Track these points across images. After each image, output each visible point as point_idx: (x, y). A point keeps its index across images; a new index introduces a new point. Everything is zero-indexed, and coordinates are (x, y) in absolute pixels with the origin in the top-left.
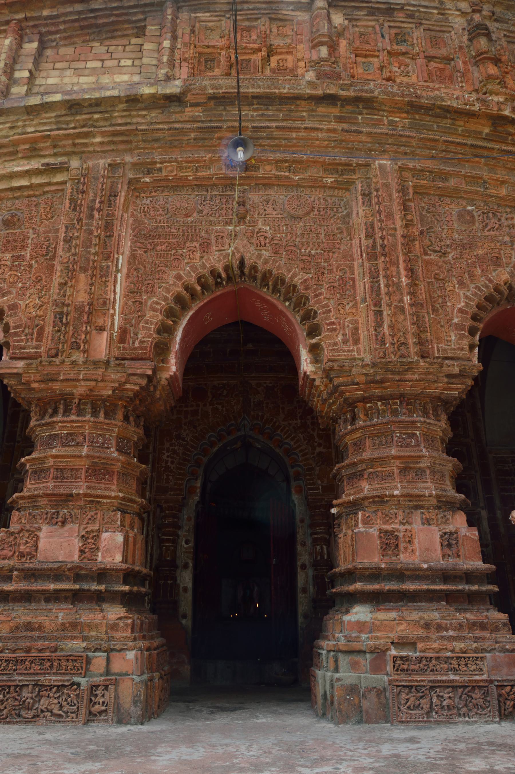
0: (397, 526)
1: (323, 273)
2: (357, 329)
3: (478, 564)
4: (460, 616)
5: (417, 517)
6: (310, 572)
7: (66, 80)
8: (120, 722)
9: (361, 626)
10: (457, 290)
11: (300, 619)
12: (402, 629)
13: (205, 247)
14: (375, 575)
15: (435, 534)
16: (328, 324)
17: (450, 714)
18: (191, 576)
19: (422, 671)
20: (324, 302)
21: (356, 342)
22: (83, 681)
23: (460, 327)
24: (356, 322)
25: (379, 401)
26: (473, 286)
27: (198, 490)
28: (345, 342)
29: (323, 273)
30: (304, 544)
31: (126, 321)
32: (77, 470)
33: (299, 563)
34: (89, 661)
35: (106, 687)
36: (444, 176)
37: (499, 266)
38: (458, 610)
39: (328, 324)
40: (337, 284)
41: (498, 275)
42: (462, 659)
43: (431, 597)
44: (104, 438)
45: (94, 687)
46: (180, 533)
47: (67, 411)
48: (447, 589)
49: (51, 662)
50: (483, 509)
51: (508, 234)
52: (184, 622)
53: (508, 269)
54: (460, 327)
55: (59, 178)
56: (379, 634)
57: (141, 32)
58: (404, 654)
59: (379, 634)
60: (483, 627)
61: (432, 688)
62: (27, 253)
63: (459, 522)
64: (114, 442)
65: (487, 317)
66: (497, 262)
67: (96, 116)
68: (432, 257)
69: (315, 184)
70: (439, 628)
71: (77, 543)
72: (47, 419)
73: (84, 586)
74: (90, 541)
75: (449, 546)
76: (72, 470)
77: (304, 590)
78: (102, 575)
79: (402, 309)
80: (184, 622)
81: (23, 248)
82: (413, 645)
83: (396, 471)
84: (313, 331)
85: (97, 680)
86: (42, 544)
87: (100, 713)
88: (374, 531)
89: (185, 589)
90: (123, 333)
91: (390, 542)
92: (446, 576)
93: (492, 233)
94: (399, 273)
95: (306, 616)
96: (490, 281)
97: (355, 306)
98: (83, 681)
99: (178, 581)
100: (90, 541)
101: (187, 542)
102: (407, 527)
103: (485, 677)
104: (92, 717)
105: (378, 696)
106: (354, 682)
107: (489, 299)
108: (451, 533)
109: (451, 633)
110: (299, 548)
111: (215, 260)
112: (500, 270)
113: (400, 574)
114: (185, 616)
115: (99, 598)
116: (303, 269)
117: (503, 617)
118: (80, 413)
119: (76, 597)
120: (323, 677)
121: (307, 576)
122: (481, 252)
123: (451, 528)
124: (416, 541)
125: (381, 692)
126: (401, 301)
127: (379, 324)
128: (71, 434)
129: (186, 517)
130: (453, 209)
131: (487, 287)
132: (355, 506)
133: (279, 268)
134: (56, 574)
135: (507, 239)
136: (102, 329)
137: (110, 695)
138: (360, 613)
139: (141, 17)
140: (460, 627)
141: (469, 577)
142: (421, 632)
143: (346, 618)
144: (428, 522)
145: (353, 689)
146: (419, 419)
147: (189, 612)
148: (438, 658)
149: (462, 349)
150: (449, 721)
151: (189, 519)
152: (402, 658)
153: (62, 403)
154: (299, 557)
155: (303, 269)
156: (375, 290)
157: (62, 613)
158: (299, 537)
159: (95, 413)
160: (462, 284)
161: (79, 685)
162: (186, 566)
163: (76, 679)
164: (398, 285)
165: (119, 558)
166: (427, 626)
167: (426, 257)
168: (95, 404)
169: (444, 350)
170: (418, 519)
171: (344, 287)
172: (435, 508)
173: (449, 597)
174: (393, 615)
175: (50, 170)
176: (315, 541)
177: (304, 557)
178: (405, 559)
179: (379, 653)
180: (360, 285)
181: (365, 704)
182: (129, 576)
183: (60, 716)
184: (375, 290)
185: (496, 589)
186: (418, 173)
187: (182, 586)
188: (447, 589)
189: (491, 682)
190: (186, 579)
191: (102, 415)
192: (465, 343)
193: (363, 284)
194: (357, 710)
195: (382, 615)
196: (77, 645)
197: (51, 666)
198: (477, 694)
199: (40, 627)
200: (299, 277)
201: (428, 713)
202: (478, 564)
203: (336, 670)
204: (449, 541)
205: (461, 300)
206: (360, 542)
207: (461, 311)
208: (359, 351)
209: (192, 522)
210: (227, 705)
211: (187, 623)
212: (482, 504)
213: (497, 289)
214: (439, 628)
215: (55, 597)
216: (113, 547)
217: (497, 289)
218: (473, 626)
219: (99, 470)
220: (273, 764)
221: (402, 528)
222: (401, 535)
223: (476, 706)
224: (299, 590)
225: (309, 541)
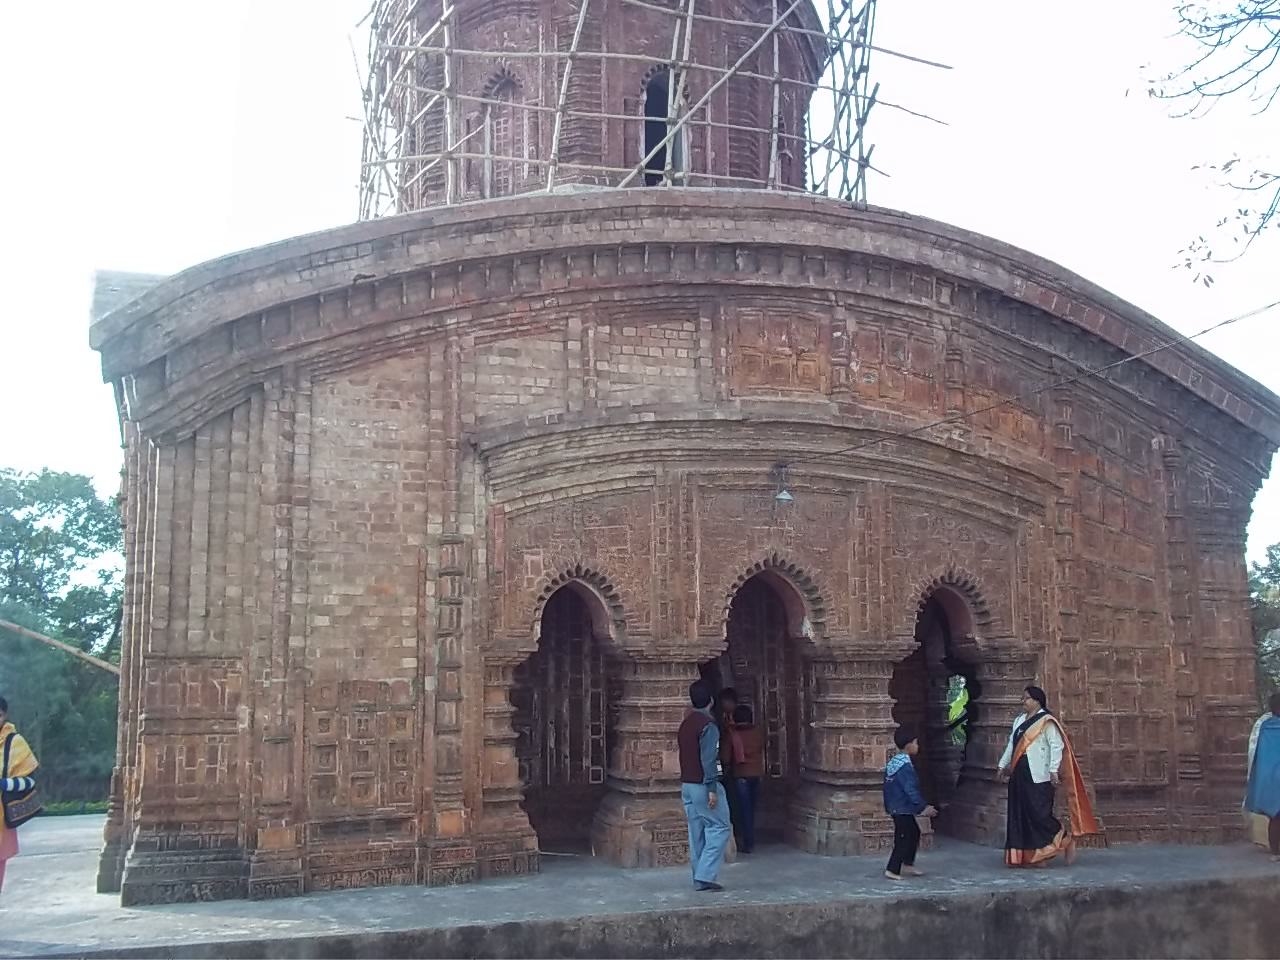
7: (635, 369)
12: (867, 807)
13: (751, 546)
14: (850, 775)
19: (875, 829)
21: (847, 623)
36: (912, 490)
53: (943, 566)
55: (648, 482)
57: (694, 317)
62: (628, 547)
67: (677, 431)
69: (827, 492)
81: (625, 542)
82: (871, 815)
84: (819, 612)
90: (702, 615)
91: (859, 755)
111: (758, 557)
113: (864, 775)
120: (817, 831)
125: (855, 840)
130: (916, 514)
138: (841, 798)
139: (694, 305)
145: (841, 839)
171: (842, 581)
174: (859, 798)
175: (642, 476)
178: (867, 766)
186: (896, 487)
193: (854, 580)
195: (854, 799)
205: (915, 590)
207: (912, 600)
217: (935, 582)
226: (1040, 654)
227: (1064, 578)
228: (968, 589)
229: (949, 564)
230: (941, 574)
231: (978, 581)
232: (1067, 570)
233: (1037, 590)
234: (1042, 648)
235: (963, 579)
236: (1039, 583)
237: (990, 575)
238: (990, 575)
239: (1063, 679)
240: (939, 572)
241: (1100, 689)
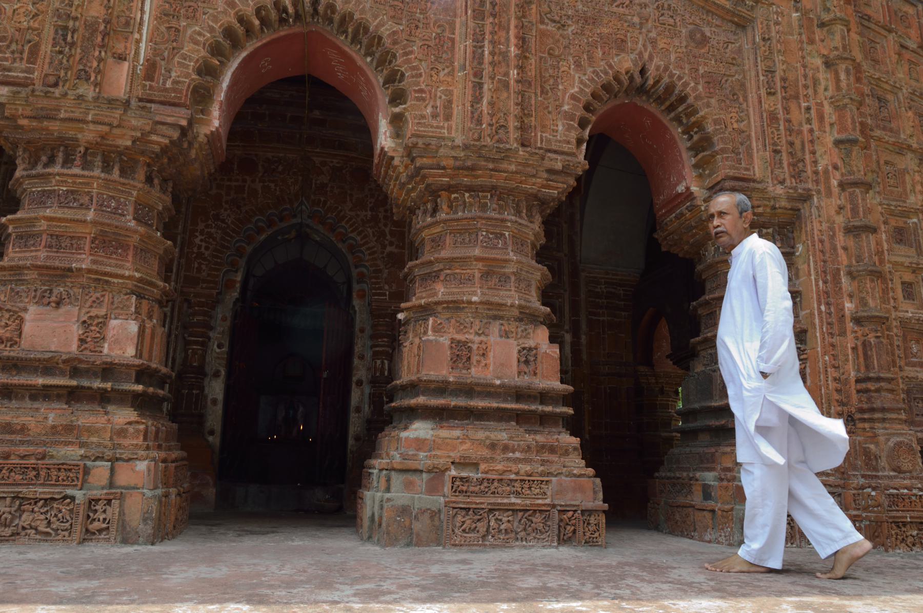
0: (471, 337)
1: (417, 27)
2: (450, 102)
3: (555, 384)
4: (529, 438)
5: (495, 328)
6: (367, 390)
8: (125, 541)
9: (420, 443)
10: (572, 72)
11: (351, 442)
12: (465, 449)
14: (442, 388)
15: (513, 348)
16: (416, 91)
17: (508, 538)
18: (222, 386)
19: (482, 493)
20: (413, 61)
21: (448, 117)
22: (79, 494)
23: (569, 116)
24: (449, 93)
25: (466, 191)
26: (591, 69)
27: (238, 285)
28: (435, 116)
29: (417, 27)
30: (362, 357)
31: (156, 52)
32: (79, 238)
33: (354, 379)
34: (87, 471)
35: (109, 502)
37: (623, 50)
38: (528, 432)
39: (416, 91)
40: (432, 43)
41: (620, 61)
42: (527, 482)
43: (501, 416)
44: (118, 201)
45: (92, 502)
46: (211, 334)
47: (68, 161)
48: (522, 409)
49: (35, 471)
50: (567, 332)
51: (638, 14)
52: (210, 439)
53: (633, 56)
54: (569, 116)
56: (439, 453)
58: (464, 474)
59: (439, 453)
60: (552, 450)
61: (491, 510)
63: (540, 337)
64: (131, 209)
65: (601, 109)
66: (621, 45)
68: (549, 28)
70: (506, 448)
71: (76, 331)
72: (39, 169)
73: (82, 383)
74: (93, 329)
75: (527, 362)
76: (72, 238)
77: (358, 410)
78: (108, 370)
79: (506, 85)
80: (210, 439)
82: (476, 465)
83: (477, 275)
84: (397, 98)
85: (97, 493)
86: (27, 328)
87: (100, 531)
88: (445, 340)
89: (214, 402)
90: (151, 68)
91: (461, 354)
92: (519, 395)
93: (621, 10)
94: (508, 39)
95: (357, 439)
96: (611, 67)
97: (451, 74)
98: (79, 494)
99: (206, 391)
100: (93, 329)
101: (219, 346)
102: (483, 338)
103: (548, 501)
104: (88, 535)
105: (432, 518)
106: (406, 503)
107: (606, 87)
108: (530, 349)
109: (517, 455)
110: (356, 361)
112: (623, 55)
113: (469, 390)
114: (212, 433)
115: (103, 398)
116: (393, 17)
117: (575, 441)
118: (86, 165)
119: (72, 395)
120: (373, 499)
121: (362, 394)
122: (606, 31)
123: (531, 343)
124: (491, 354)
125: (434, 514)
126: (507, 74)
127: (477, 99)
128: (72, 192)
129: (220, 316)
131: (606, 73)
132: (426, 310)
133: (363, 11)
134: (47, 366)
135: (636, 20)
136: (121, 58)
137: (113, 512)
138: (420, 429)
140: (529, 449)
141: (544, 397)
142: (486, 453)
143: (404, 434)
144: (506, 335)
145: (404, 510)
146: (510, 217)
147: (218, 428)
148: (500, 480)
149: (568, 142)
150: (505, 545)
151: (224, 319)
152: (462, 479)
153: (62, 150)
154: (354, 372)
155: (393, 17)
156: (478, 57)
157: (53, 414)
158: (357, 349)
159: (107, 167)
160: (578, 65)
161: (73, 498)
162: (216, 375)
163: (69, 492)
164: (505, 55)
165: (131, 351)
166: (493, 446)
167: (542, 27)
168: (108, 156)
169: (549, 141)
170: (496, 330)
171: (441, 48)
172: (515, 320)
173: (520, 418)
174: (457, 433)
176: (376, 355)
177: (360, 372)
178: (476, 373)
179: (437, 472)
180: (460, 48)
181: (417, 526)
182: (143, 374)
183: (48, 534)
184: (478, 57)
185: (571, 411)
187: (210, 397)
188: (522, 409)
189: (554, 506)
190: (216, 389)
191: (116, 172)
192: (573, 135)
193: (463, 47)
194: (407, 532)
195: (444, 433)
196: (71, 453)
197: (37, 476)
198: (538, 519)
199: (23, 429)
200: (386, 26)
201: (484, 537)
202: (555, 384)
203: (388, 490)
204: (528, 357)
205: (575, 84)
206: (427, 353)
207: (573, 97)
208: (450, 129)
209: (228, 323)
210: (258, 529)
211: (215, 440)
212: (567, 327)
213: (616, 78)
214: (506, 448)
215: (45, 394)
216: (124, 338)
217: (616, 78)
218: (541, 448)
219: (108, 241)
220: (308, 582)
221: (477, 339)
222: (475, 347)
223: (535, 530)
224: (352, 408)
225: (369, 355)
226: (805, 209)
227: (838, 88)
228: (673, 100)
229: (640, 54)
230: (628, 65)
231: (694, 89)
232: (843, 76)
233: (793, 106)
234: (806, 198)
235: (666, 80)
236: (797, 97)
237: (713, 82)
238: (713, 82)
239: (845, 249)
240: (625, 63)
241: (908, 277)
